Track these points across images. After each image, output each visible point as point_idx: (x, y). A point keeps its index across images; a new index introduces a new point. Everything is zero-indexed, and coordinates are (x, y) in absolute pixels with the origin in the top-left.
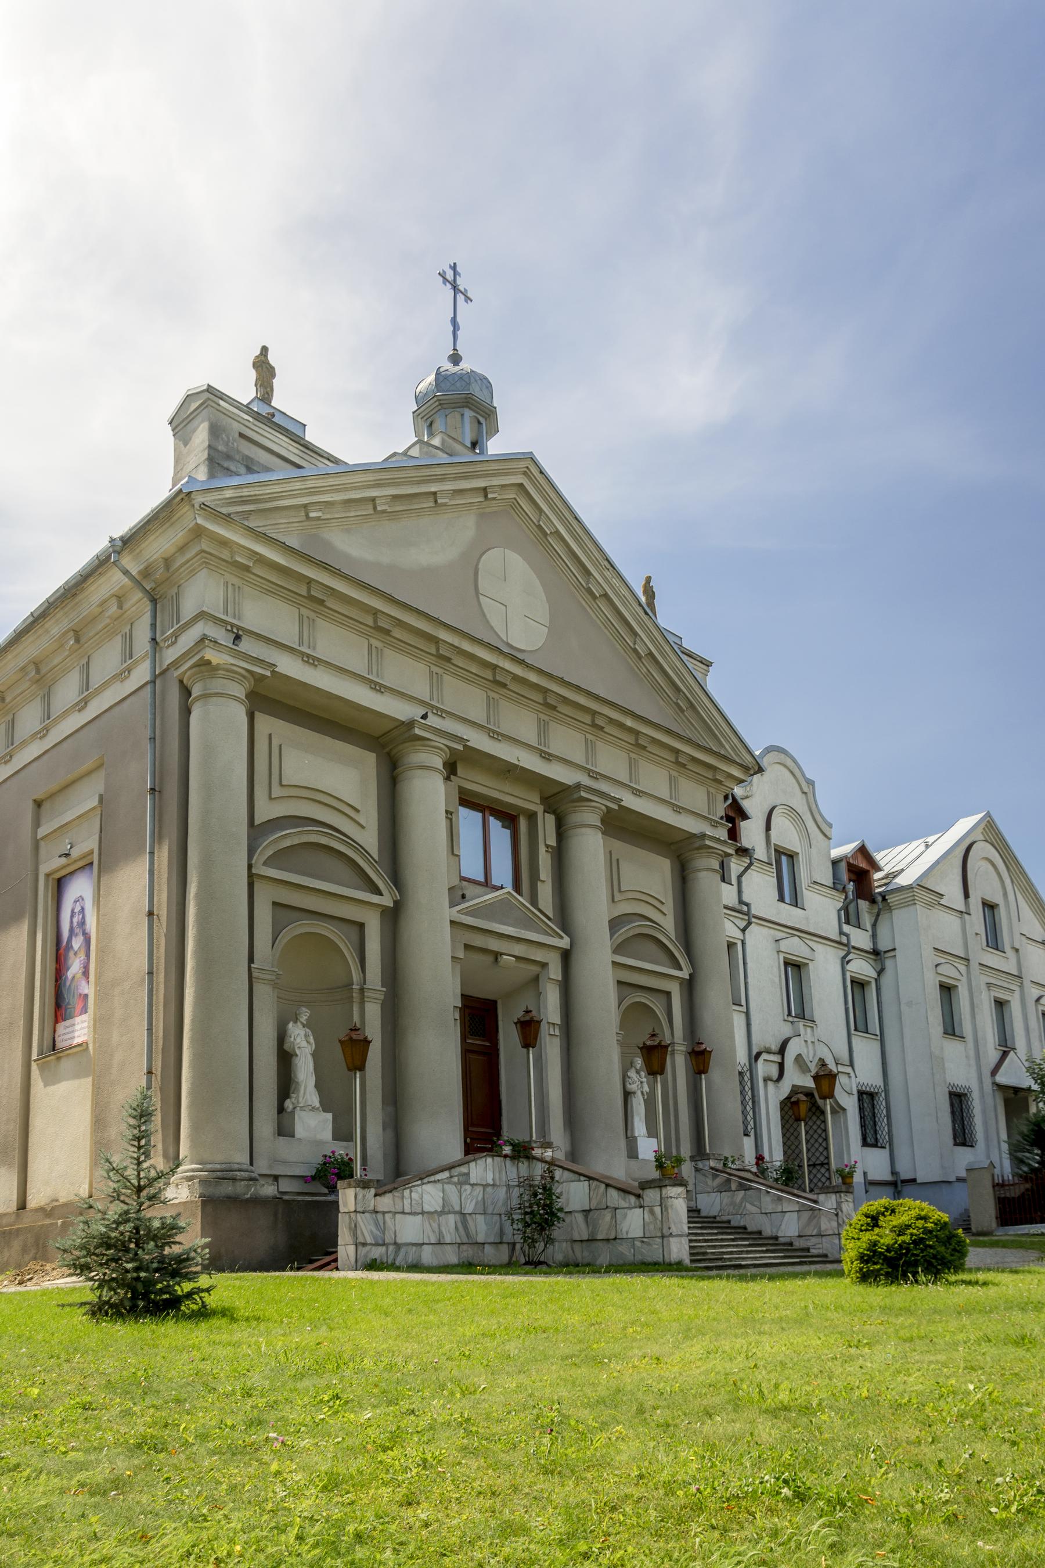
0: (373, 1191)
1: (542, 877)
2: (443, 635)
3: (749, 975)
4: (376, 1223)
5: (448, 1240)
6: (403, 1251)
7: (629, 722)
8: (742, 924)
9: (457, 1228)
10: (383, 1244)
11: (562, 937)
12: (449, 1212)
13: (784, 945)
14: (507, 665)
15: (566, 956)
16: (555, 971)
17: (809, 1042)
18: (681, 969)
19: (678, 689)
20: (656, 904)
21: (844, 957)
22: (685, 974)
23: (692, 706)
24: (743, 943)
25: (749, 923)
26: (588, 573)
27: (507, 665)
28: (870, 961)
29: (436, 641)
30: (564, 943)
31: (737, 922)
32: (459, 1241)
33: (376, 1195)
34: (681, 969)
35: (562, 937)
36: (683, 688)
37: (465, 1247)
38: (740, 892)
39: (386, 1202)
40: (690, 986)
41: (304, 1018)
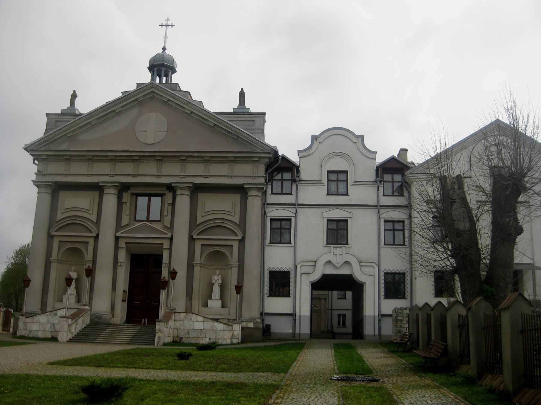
0: (25, 317)
1: (165, 214)
2: (108, 154)
3: (298, 230)
4: (25, 325)
5: (47, 330)
6: (32, 332)
7: (196, 155)
8: (294, 210)
9: (51, 327)
10: (26, 330)
11: (168, 234)
12: (49, 323)
13: (325, 215)
14: (135, 154)
15: (171, 239)
16: (166, 245)
17: (338, 255)
18: (238, 236)
19: (231, 133)
20: (228, 213)
21: (379, 212)
22: (240, 237)
23: (238, 137)
24: (296, 217)
25: (296, 210)
26: (184, 108)
27: (135, 154)
28: (401, 210)
29: (108, 156)
30: (169, 235)
31: (291, 210)
32: (51, 330)
33: (26, 318)
34: (237, 235)
35: (168, 234)
36: (232, 132)
37: (54, 332)
38: (297, 196)
39: (28, 320)
40: (242, 241)
41: (73, 270)
